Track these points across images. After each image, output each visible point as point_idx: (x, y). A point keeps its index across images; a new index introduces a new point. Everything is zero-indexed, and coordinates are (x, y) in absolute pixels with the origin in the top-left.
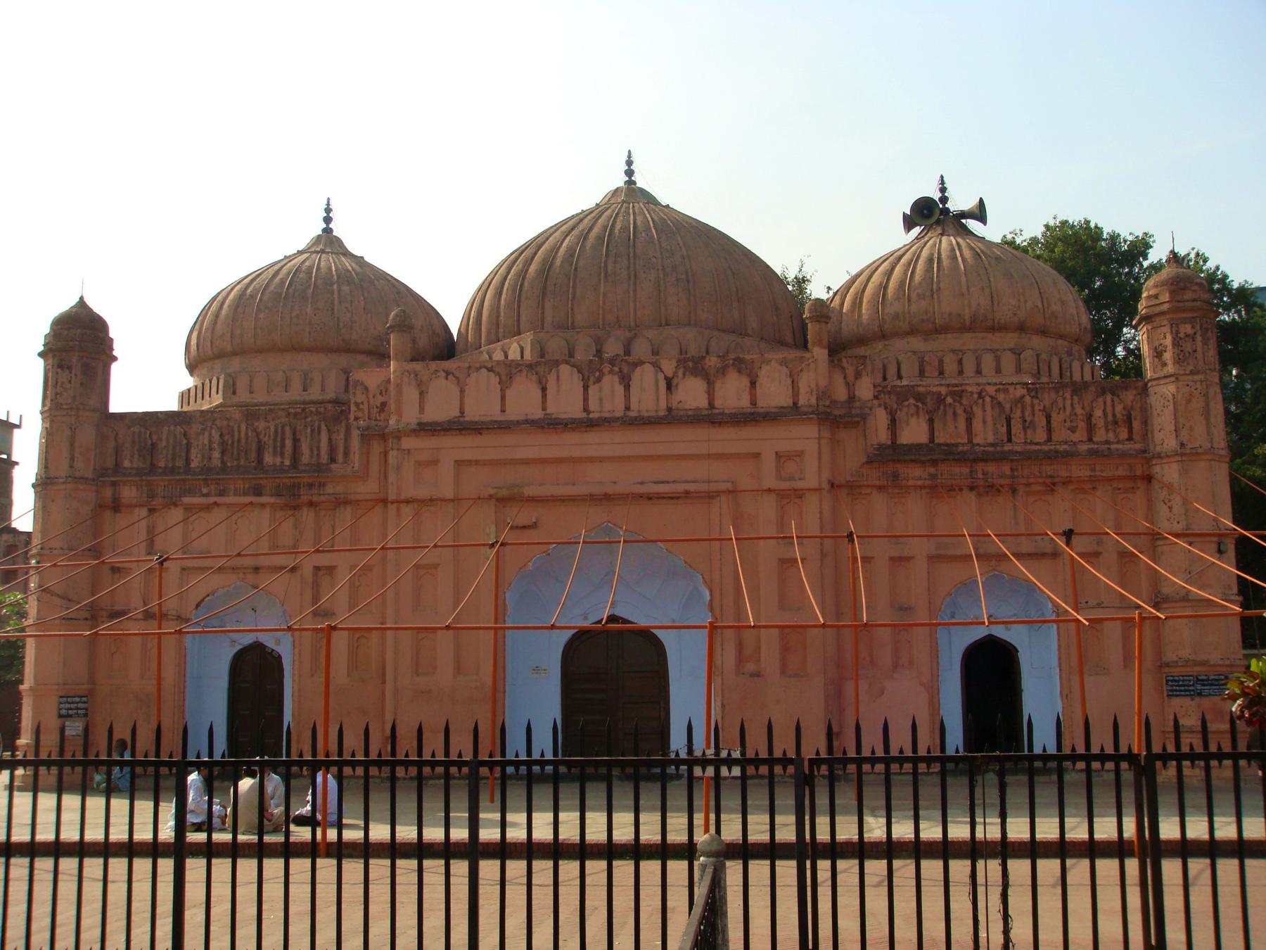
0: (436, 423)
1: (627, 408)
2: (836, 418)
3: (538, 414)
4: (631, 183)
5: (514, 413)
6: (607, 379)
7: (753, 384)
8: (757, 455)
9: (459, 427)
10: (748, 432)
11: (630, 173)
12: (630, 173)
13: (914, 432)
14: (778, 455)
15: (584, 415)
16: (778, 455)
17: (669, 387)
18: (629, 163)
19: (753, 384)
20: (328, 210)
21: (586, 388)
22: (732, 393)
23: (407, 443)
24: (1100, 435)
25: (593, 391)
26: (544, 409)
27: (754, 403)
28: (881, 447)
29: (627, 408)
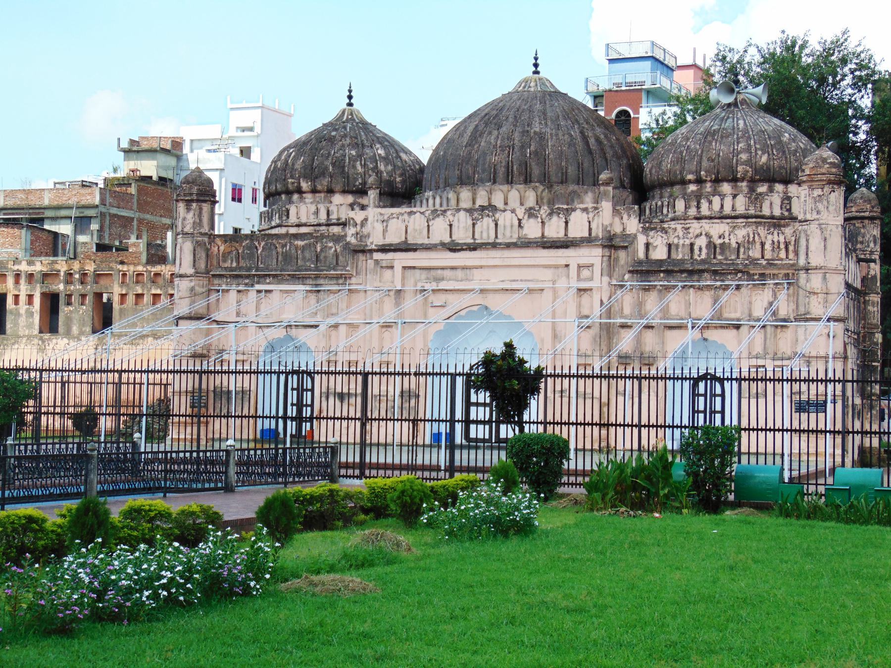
0: (391, 245)
1: (496, 237)
2: (612, 243)
3: (447, 240)
4: (536, 72)
5: (435, 239)
6: (486, 219)
7: (567, 223)
8: (567, 266)
9: (406, 247)
10: (561, 252)
11: (536, 65)
12: (536, 65)
13: (659, 253)
14: (579, 267)
15: (472, 241)
16: (579, 267)
17: (520, 226)
18: (536, 59)
19: (567, 223)
20: (350, 91)
21: (474, 225)
22: (555, 229)
23: (377, 256)
24: (768, 255)
25: (476, 226)
26: (451, 237)
27: (566, 235)
28: (640, 262)
29: (496, 237)
